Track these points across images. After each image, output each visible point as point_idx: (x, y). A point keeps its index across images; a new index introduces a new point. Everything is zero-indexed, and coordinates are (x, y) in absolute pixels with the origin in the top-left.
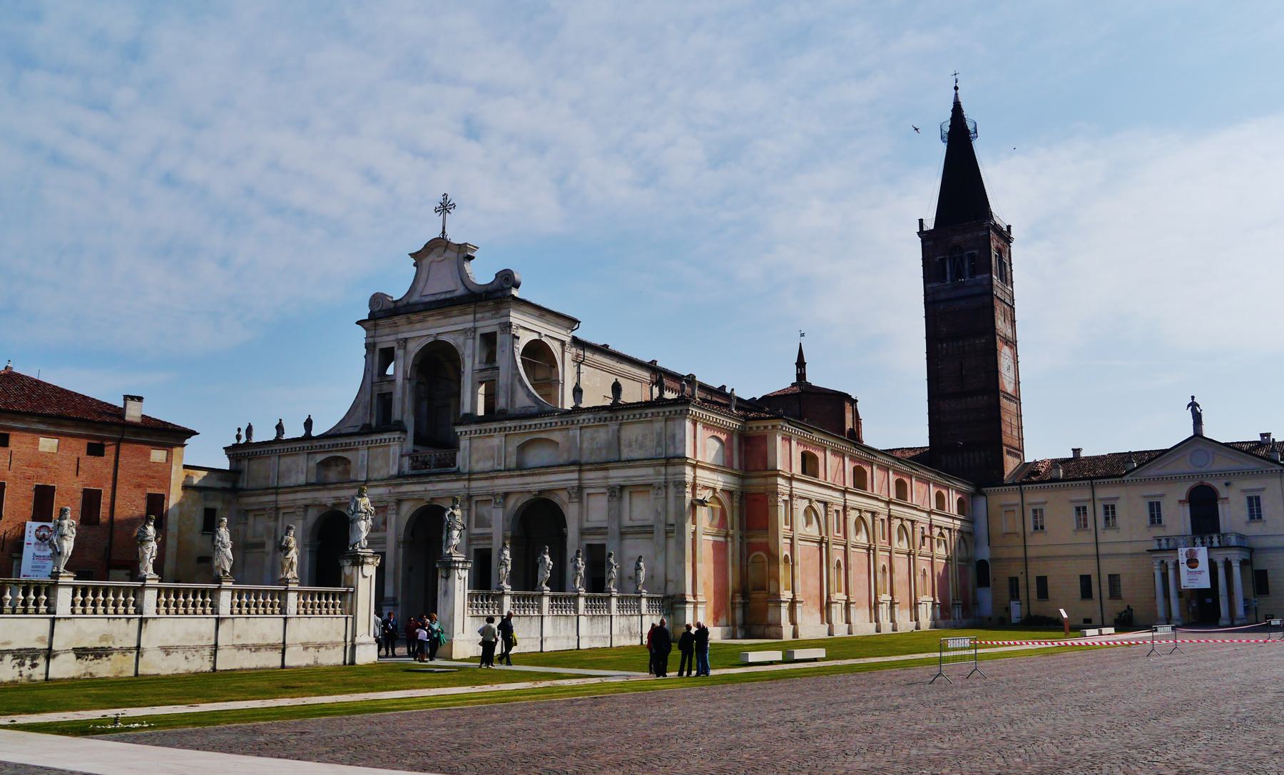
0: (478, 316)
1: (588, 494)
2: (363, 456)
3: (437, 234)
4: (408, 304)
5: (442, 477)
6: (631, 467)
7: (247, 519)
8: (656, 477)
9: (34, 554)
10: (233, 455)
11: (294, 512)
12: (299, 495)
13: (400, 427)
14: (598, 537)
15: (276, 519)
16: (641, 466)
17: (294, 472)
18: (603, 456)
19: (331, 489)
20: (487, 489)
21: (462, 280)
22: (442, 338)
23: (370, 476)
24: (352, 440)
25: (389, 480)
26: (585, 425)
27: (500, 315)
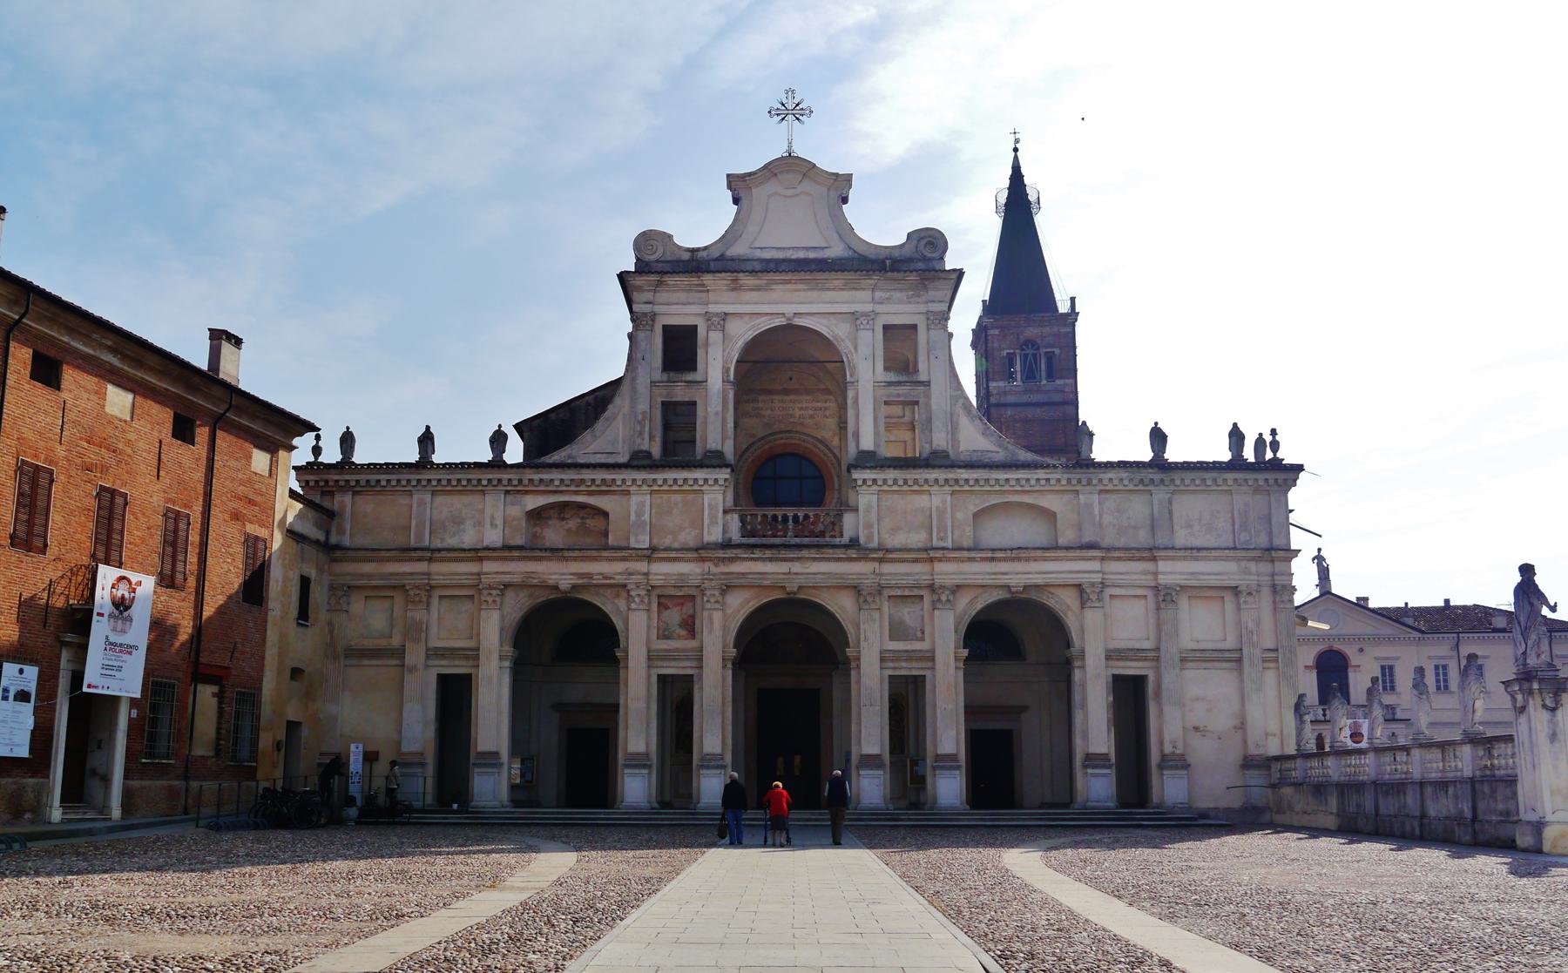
0: (878, 294)
1: (1110, 596)
2: (643, 503)
3: (779, 152)
4: (722, 258)
5: (829, 553)
6: (1197, 559)
7: (348, 604)
8: (1243, 577)
9: (107, 637)
10: (317, 482)
11: (471, 597)
12: (489, 566)
13: (714, 460)
14: (1140, 664)
15: (428, 604)
16: (1216, 559)
17: (469, 523)
18: (1143, 538)
19: (566, 559)
20: (917, 577)
21: (838, 233)
22: (799, 321)
23: (655, 541)
24: (618, 476)
25: (701, 551)
26: (1110, 487)
27: (923, 298)
